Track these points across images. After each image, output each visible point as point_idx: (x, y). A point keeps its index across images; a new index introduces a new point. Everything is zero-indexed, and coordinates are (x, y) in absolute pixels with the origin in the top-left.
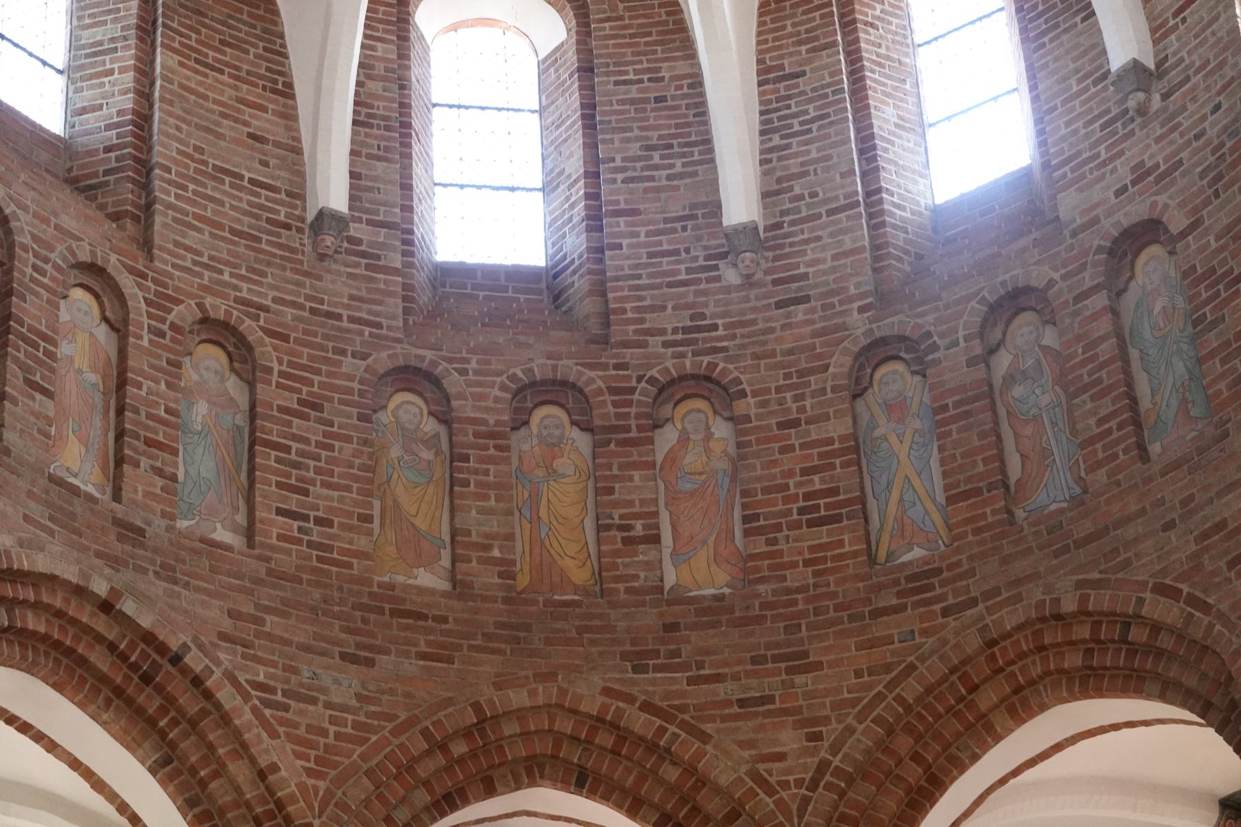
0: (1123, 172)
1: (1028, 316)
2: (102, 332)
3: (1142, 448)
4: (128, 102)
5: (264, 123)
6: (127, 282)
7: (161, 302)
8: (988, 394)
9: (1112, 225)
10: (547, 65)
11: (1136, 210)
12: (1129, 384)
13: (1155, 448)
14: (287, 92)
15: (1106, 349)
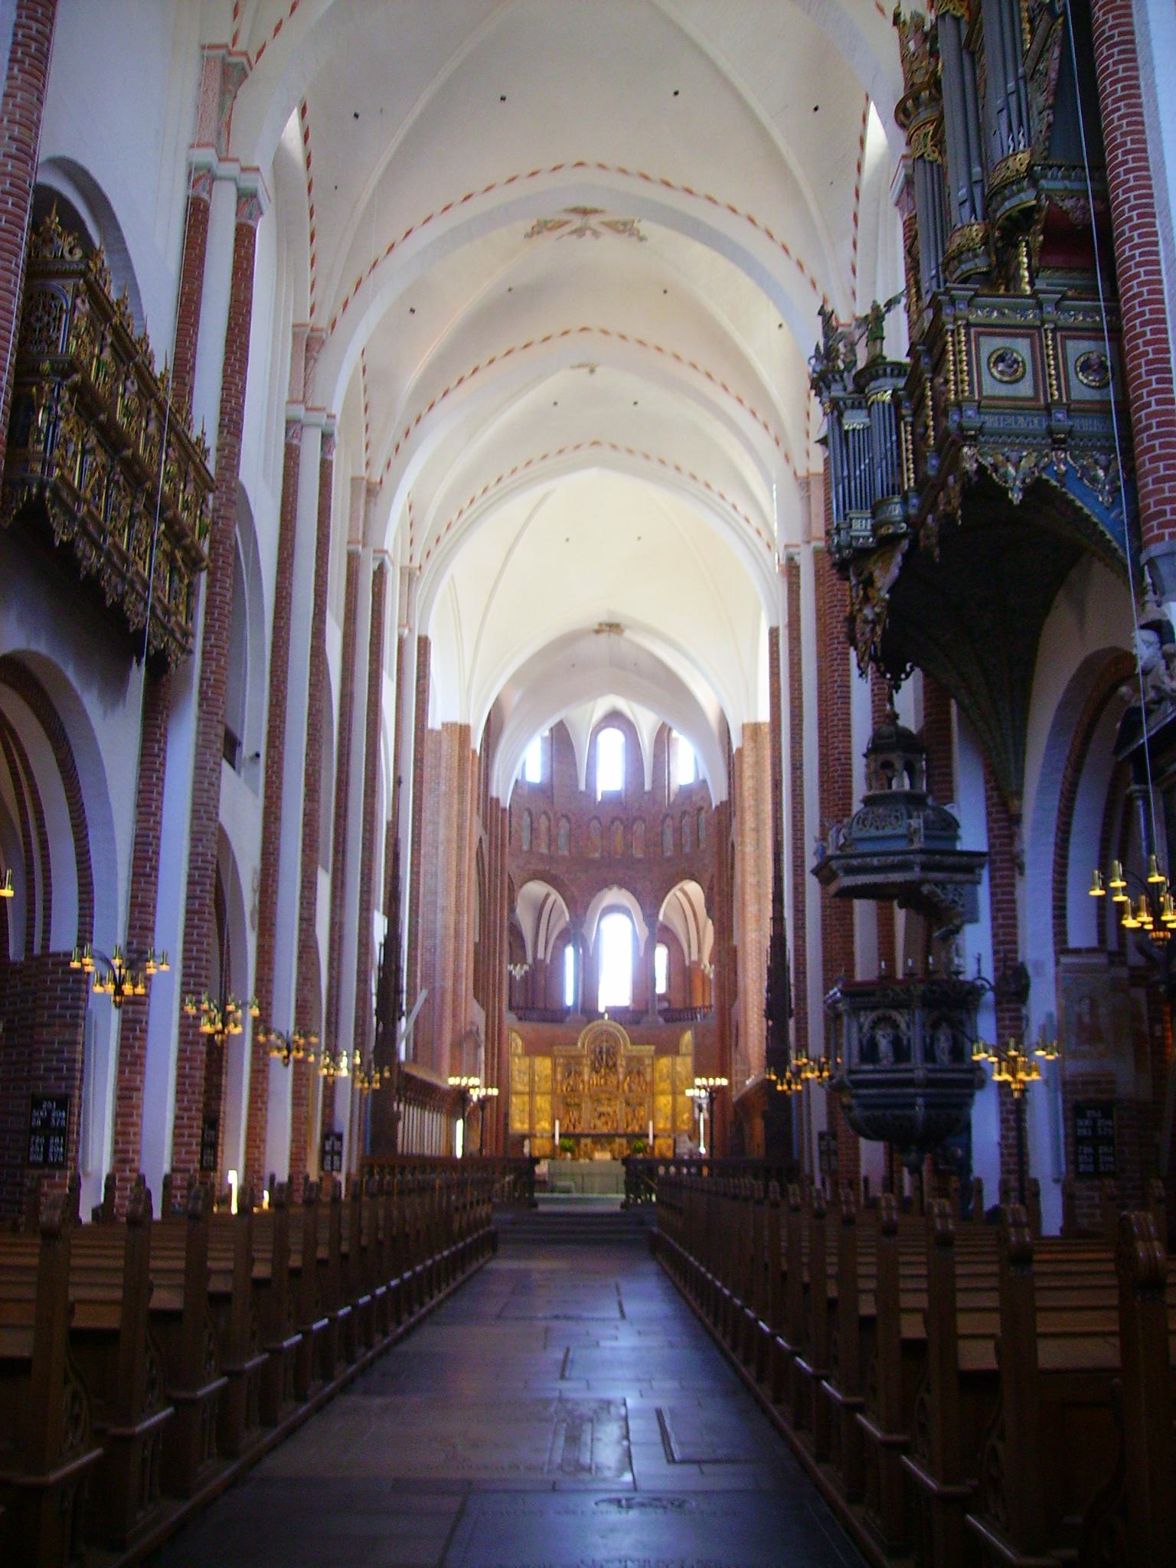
7: (555, 814)
8: (681, 828)
11: (701, 803)
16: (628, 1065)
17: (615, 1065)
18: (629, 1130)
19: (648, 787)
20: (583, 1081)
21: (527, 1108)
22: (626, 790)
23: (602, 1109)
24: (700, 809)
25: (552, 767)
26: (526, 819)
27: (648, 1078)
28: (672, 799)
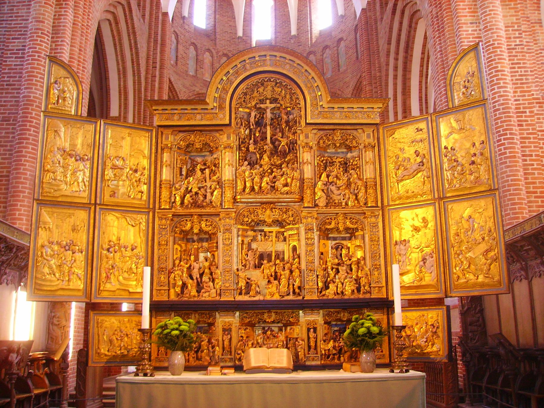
0: (340, 29)
1: (328, 49)
2: (210, 58)
3: (339, 70)
4: (213, 23)
5: (231, 23)
6: (213, 50)
7: (217, 53)
8: (322, 60)
9: (336, 39)
10: (272, 8)
11: (340, 36)
12: (338, 60)
13: (341, 70)
14: (235, 18)
15: (336, 55)
16: (322, 149)
17: (292, 146)
18: (330, 293)
19: (294, 32)
20: (219, 182)
21: (82, 239)
22: (276, 38)
23: (260, 246)
24: (341, 39)
25: (215, 18)
26: (192, 52)
27: (368, 173)
28: (313, 41)
